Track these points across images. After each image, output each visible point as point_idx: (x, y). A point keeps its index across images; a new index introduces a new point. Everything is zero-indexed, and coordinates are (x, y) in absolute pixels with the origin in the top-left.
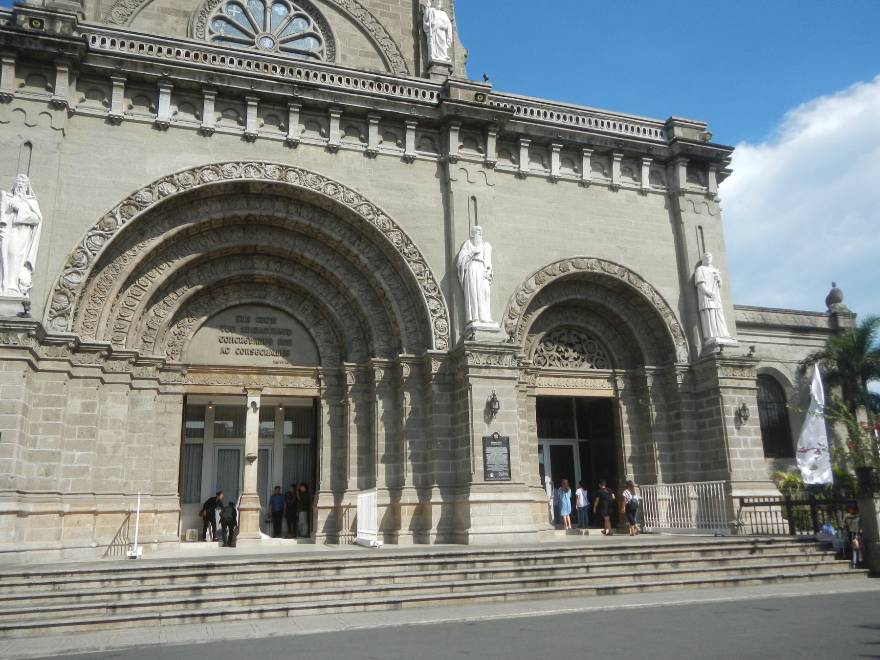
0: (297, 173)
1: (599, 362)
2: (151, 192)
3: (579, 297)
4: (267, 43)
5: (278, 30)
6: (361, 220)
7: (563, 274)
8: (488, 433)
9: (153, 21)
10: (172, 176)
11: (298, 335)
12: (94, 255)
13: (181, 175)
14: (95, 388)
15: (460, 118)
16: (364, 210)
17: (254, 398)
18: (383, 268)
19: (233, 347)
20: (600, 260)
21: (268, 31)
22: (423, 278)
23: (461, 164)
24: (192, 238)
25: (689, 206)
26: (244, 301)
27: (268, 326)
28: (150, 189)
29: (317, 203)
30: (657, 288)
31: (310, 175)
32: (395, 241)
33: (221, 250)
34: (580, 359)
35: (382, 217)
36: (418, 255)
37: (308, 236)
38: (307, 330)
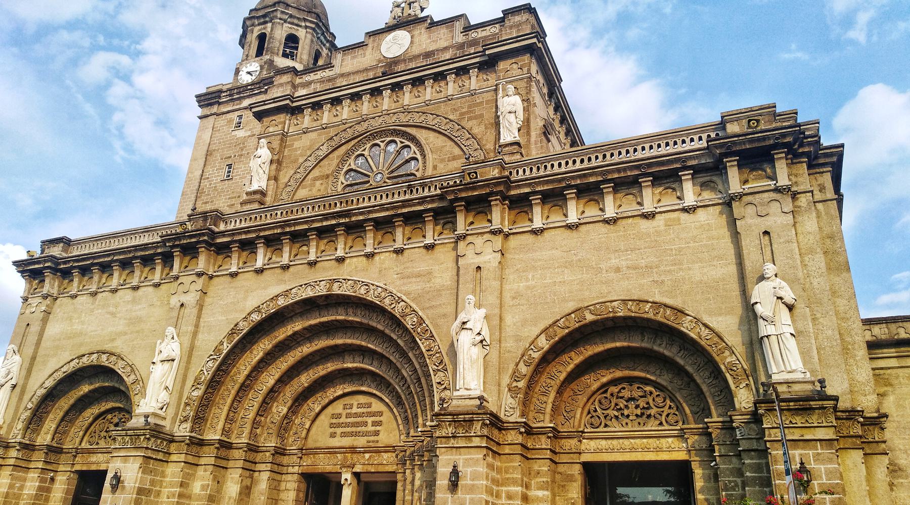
1: (670, 418)
3: (618, 344)
4: (379, 177)
7: (577, 325)
9: (307, 189)
11: (387, 417)
14: (209, 473)
15: (462, 199)
16: (387, 301)
17: (347, 476)
19: (339, 431)
20: (624, 301)
23: (469, 239)
25: (751, 210)
26: (346, 391)
27: (365, 410)
30: (706, 319)
34: (645, 416)
35: (402, 303)
37: (370, 331)
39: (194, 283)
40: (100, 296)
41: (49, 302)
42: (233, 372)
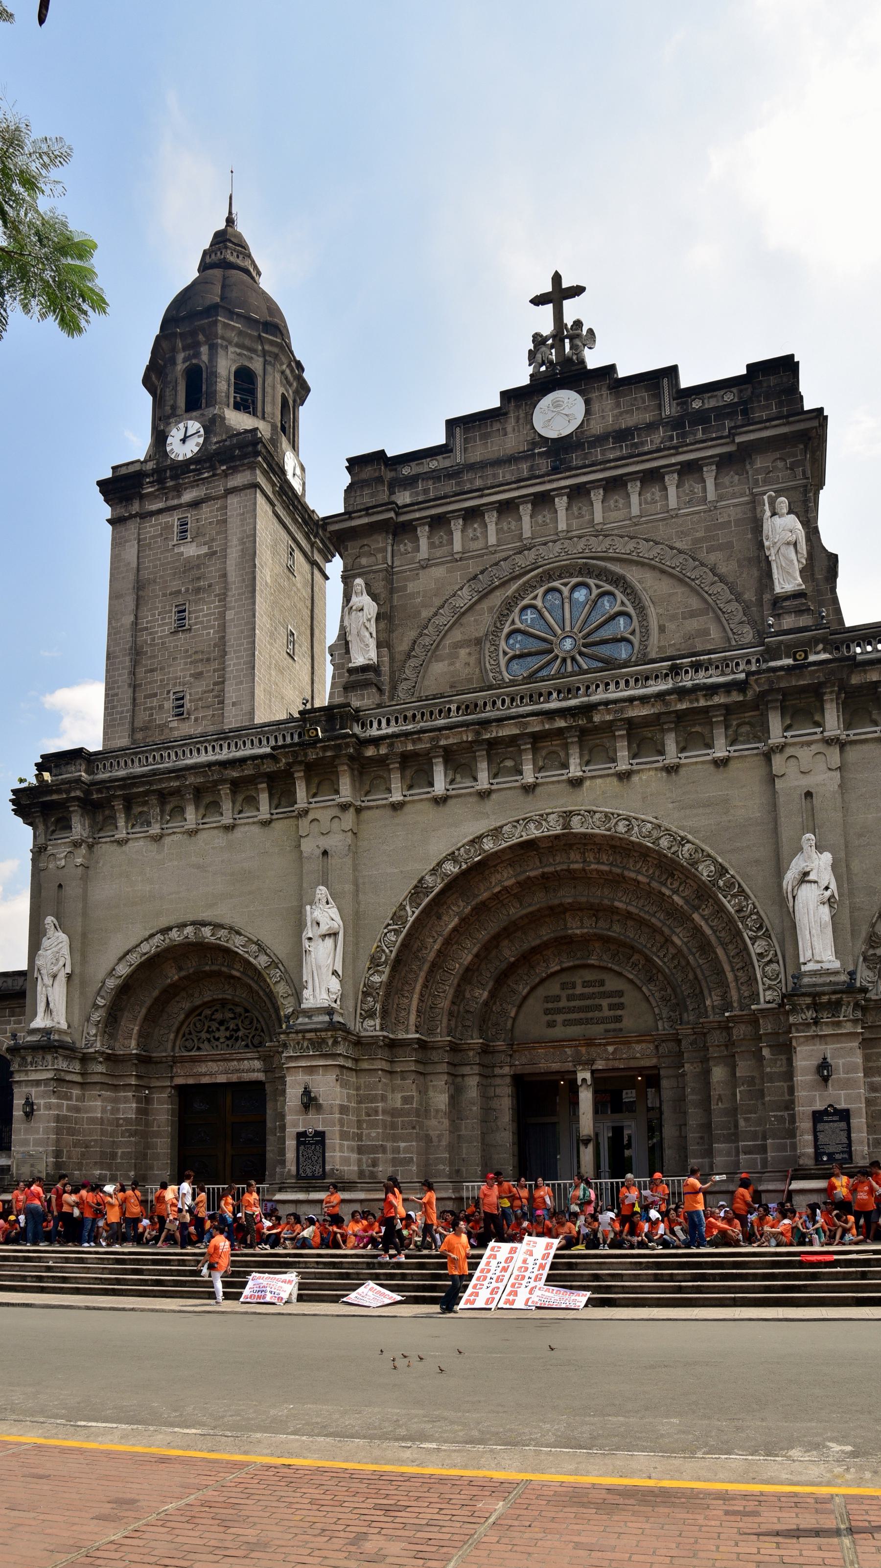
0: (583, 816)
2: (435, 874)
5: (580, 622)
6: (665, 856)
8: (819, 1106)
10: (453, 853)
12: (391, 951)
13: (462, 849)
18: (704, 907)
21: (568, 629)
22: (742, 914)
24: (493, 909)
28: (433, 871)
29: (613, 843)
31: (597, 816)
32: (705, 874)
33: (526, 915)
35: (688, 846)
36: (737, 886)
38: (640, 989)
39: (336, 820)
40: (167, 840)
41: (84, 851)
42: (416, 946)
